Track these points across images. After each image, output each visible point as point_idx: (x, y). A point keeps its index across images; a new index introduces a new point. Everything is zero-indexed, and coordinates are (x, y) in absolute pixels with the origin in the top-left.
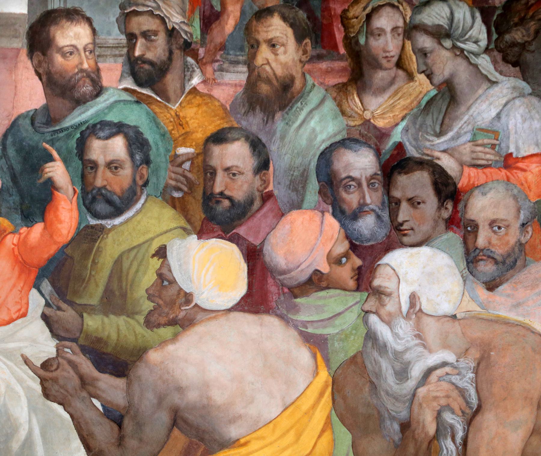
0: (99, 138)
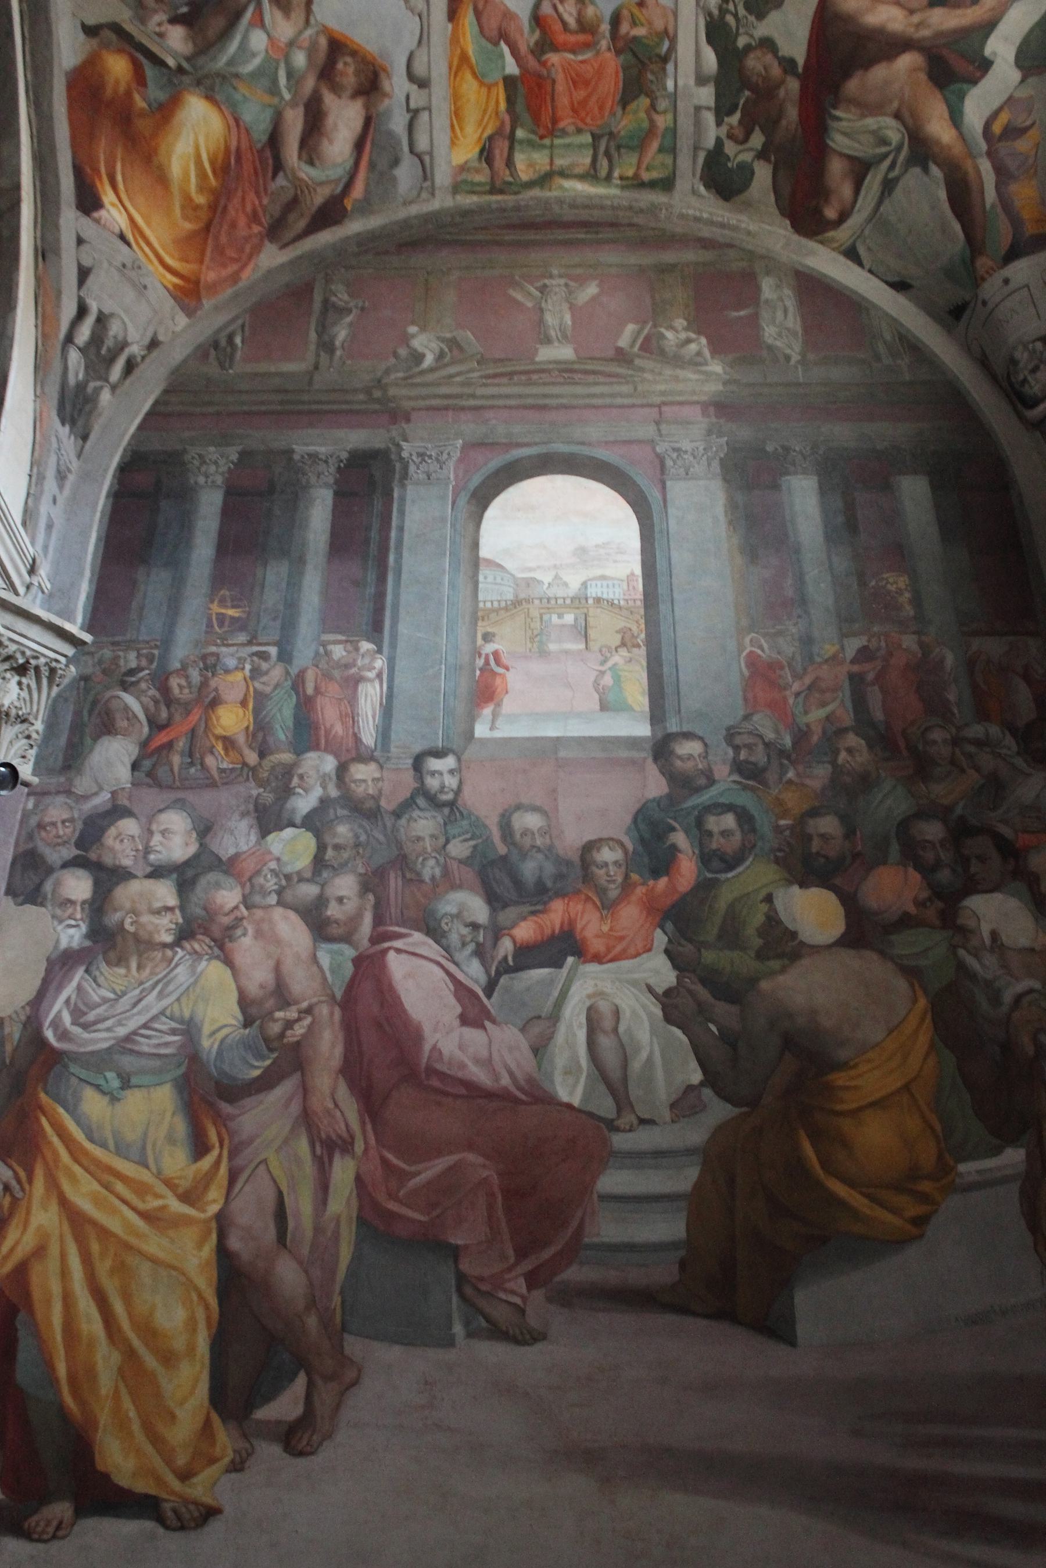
0: (714, 814)
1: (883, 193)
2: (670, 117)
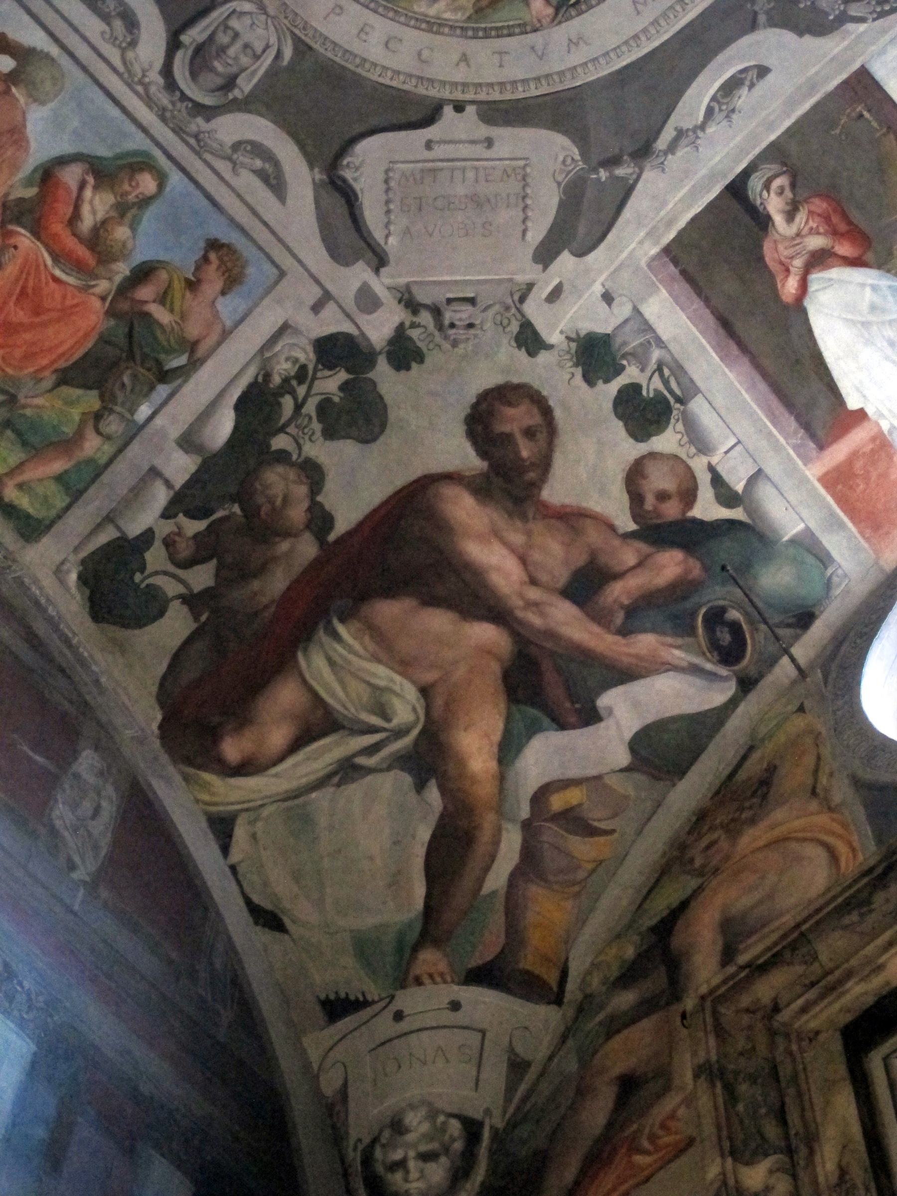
1: (329, 776)
2: (108, 449)
